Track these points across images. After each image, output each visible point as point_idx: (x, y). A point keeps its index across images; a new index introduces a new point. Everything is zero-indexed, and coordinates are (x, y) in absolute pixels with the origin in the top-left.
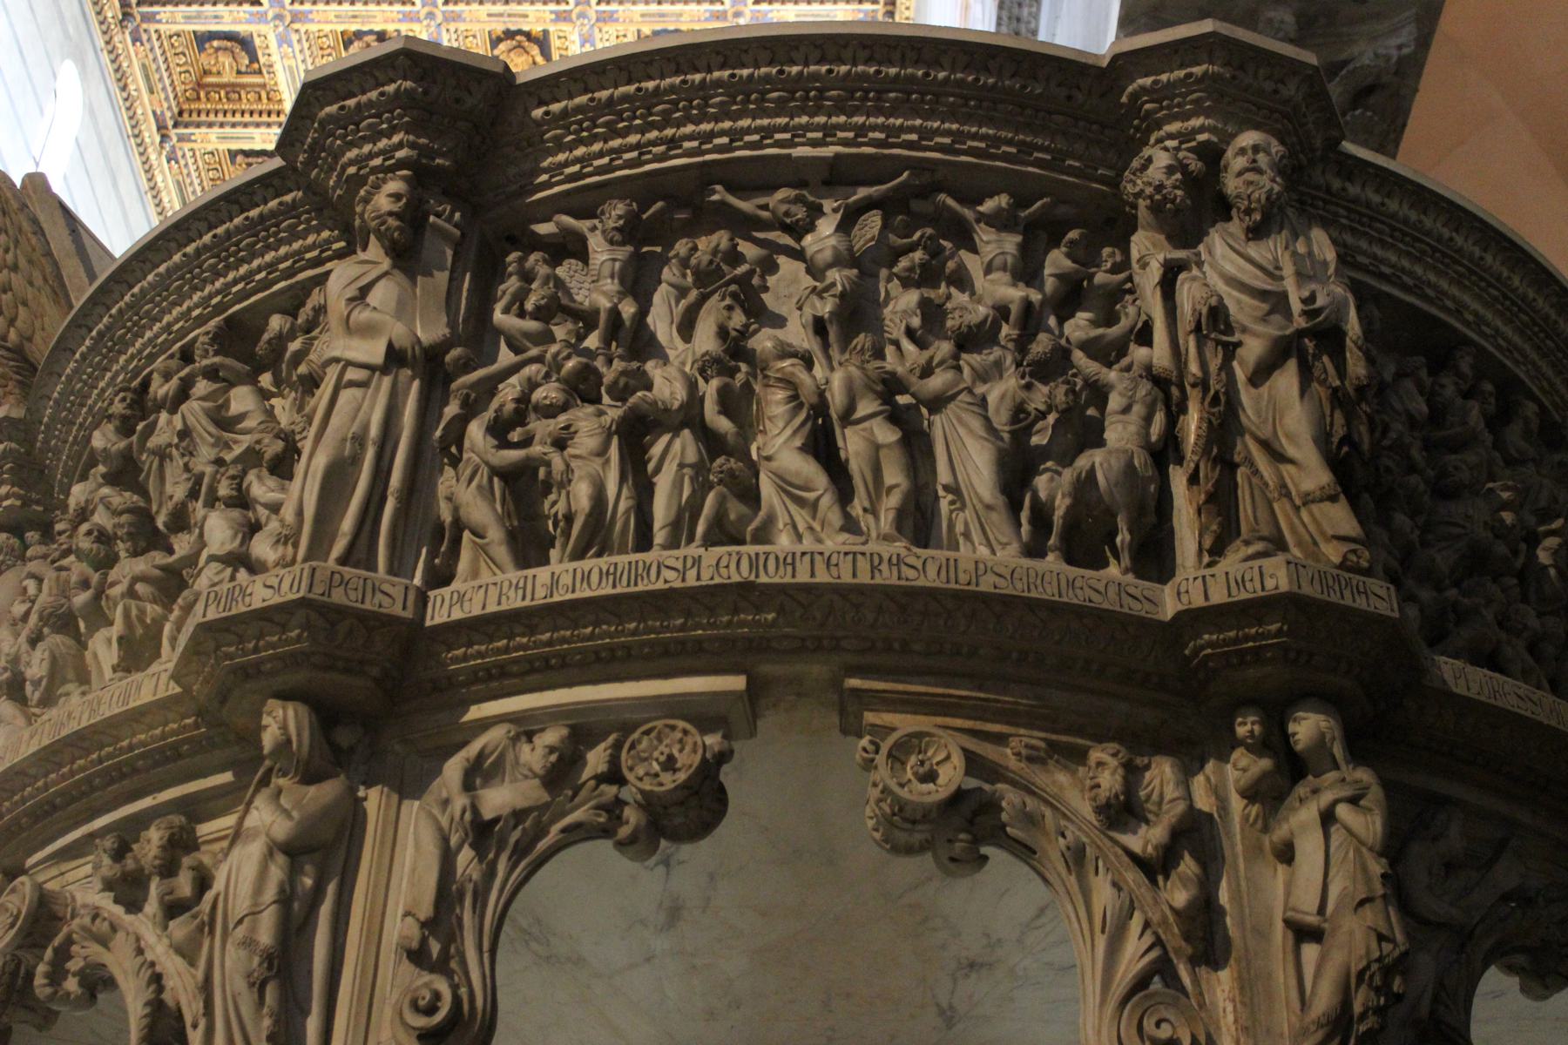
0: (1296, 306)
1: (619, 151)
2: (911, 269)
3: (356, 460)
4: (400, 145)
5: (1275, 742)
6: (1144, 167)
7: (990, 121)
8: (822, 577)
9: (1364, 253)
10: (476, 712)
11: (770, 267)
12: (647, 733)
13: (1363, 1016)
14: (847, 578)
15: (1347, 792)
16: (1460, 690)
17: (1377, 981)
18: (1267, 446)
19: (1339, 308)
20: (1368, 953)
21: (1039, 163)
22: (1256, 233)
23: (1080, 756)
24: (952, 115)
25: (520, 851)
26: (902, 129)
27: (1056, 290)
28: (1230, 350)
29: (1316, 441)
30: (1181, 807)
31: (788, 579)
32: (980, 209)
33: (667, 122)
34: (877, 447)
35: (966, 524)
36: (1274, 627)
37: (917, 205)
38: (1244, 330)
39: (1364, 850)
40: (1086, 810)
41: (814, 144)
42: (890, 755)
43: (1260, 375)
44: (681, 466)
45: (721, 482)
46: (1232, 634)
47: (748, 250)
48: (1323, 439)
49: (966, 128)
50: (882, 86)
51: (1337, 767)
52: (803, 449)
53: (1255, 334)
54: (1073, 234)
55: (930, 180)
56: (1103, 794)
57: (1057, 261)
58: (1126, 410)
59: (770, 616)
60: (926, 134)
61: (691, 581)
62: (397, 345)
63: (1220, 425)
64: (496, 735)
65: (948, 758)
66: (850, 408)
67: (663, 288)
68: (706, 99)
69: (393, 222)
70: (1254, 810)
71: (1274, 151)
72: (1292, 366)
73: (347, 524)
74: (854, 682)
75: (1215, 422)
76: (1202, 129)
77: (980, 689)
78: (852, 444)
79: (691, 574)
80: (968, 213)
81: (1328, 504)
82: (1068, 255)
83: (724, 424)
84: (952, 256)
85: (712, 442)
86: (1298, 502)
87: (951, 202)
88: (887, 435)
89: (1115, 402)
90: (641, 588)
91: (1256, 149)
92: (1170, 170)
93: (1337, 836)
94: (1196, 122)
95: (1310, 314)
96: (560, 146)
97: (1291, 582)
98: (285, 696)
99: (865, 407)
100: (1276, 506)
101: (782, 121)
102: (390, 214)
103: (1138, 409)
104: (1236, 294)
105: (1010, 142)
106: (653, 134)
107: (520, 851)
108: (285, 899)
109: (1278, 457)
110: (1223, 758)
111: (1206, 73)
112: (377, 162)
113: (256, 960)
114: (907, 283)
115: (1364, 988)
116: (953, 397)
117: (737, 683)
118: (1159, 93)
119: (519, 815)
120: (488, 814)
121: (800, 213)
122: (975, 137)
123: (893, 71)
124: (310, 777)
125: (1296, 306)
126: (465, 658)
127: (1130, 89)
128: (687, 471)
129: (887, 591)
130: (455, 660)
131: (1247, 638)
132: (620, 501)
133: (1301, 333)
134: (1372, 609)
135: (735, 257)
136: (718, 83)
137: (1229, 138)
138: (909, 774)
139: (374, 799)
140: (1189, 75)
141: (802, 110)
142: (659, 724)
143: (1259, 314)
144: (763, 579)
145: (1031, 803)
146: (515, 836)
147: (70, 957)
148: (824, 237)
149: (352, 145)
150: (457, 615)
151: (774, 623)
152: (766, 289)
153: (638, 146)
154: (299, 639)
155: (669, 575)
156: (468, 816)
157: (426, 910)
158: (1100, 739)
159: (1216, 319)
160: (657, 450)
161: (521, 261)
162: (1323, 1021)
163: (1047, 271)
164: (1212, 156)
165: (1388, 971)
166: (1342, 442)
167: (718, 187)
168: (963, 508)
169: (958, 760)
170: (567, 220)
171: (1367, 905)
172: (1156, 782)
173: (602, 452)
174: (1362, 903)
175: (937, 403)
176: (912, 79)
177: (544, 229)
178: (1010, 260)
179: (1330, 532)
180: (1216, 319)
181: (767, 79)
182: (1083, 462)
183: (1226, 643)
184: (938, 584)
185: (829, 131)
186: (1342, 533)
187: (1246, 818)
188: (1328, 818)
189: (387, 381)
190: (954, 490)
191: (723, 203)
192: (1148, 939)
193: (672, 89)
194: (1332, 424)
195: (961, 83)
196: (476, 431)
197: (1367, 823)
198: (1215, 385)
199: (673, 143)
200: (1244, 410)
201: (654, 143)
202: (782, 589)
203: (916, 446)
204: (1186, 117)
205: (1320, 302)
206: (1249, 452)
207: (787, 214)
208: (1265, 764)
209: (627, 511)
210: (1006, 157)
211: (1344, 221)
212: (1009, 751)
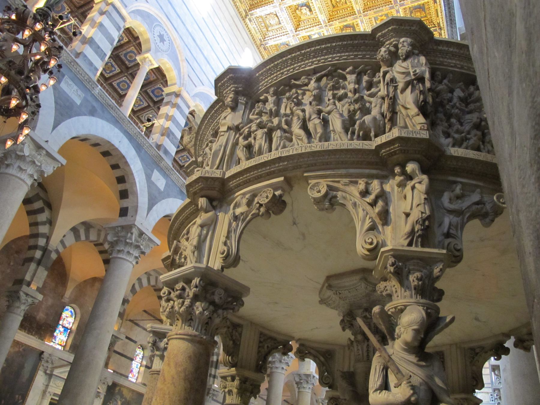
0: (412, 74)
1: (272, 78)
2: (330, 87)
3: (220, 150)
4: (232, 87)
5: (404, 173)
6: (380, 52)
7: (347, 52)
8: (295, 152)
9: (446, 62)
10: (237, 194)
11: (304, 94)
12: (264, 192)
13: (418, 231)
14: (300, 152)
15: (418, 181)
16: (456, 154)
17: (421, 223)
18: (403, 106)
19: (424, 72)
20: (418, 216)
21: (359, 58)
22: (405, 60)
23: (356, 183)
24: (338, 52)
25: (243, 220)
26: (328, 58)
27: (366, 85)
28: (396, 88)
29: (414, 103)
30: (378, 190)
31: (288, 154)
32: (346, 71)
33: (281, 69)
34: (315, 125)
35: (337, 138)
36: (397, 145)
37: (334, 74)
38: (399, 82)
39: (421, 194)
40: (358, 195)
41: (310, 66)
42: (310, 188)
43: (403, 90)
44: (277, 137)
45: (284, 139)
46: (388, 149)
47: (299, 92)
48: (416, 103)
49: (342, 54)
50: (322, 50)
51: (418, 176)
52: (300, 128)
53: (401, 82)
54: (369, 72)
55: (336, 67)
56: (360, 190)
57: (365, 78)
58: (375, 106)
59: (286, 163)
60: (333, 58)
61: (269, 159)
62: (229, 126)
63: (392, 104)
64: (239, 198)
65: (323, 187)
66: (310, 117)
67: (284, 103)
68: (287, 63)
69: (230, 103)
70: (400, 189)
71: (408, 41)
72: (410, 87)
73: (218, 162)
74: (305, 174)
75: (390, 103)
76: (394, 41)
77: (333, 171)
78: (310, 126)
79: (269, 157)
80: (344, 73)
81: (417, 116)
82: (368, 77)
83: (285, 127)
84: (342, 83)
85: (285, 131)
86: (411, 118)
87: (341, 71)
88: (317, 121)
89: (373, 105)
90: (260, 162)
91: (403, 42)
92: (385, 51)
93: (416, 191)
94: (392, 40)
95: (414, 75)
96: (263, 80)
97: (399, 134)
98: (202, 197)
99: (313, 117)
100: (406, 120)
101: (303, 63)
102: (230, 101)
103: (378, 106)
104: (399, 75)
105: (352, 55)
106: (278, 73)
107: (243, 220)
108: (200, 236)
109: (406, 108)
110: (394, 178)
111: (392, 28)
112: (228, 92)
113: (193, 247)
114: (330, 90)
115: (418, 225)
116: (333, 111)
117: (282, 179)
118: (383, 36)
119: (242, 214)
120: (237, 214)
121: (306, 81)
122: (344, 56)
123: (323, 46)
124: (206, 212)
125: (412, 74)
126: (233, 183)
127: (377, 36)
128: (279, 138)
129: (308, 153)
130: (231, 184)
131: (392, 149)
132: (265, 147)
133: (413, 80)
134: (421, 137)
136: (289, 59)
137: (399, 41)
138: (315, 192)
139: (221, 215)
140: (389, 30)
141: (307, 59)
142: (266, 190)
143: (403, 78)
144: (283, 155)
145: (344, 194)
146: (242, 217)
147: (182, 255)
148: (313, 84)
149: (225, 90)
150: (230, 175)
151: (287, 165)
152: (303, 99)
153: (276, 76)
154: (201, 185)
155: (265, 158)
156: (232, 215)
157: (226, 235)
158: (361, 178)
159: (393, 80)
160: (273, 136)
161: (258, 105)
162: (407, 233)
163: (364, 81)
164: (396, 46)
165: (424, 221)
166: (422, 101)
167: (292, 80)
168: (336, 135)
169: (326, 187)
170: (265, 95)
171: (419, 206)
172: (374, 186)
173: (262, 138)
174: (418, 205)
175: (329, 113)
176: (328, 47)
177: (262, 98)
178: (353, 80)
179: (418, 122)
180: (393, 80)
181: (298, 55)
182: (363, 119)
183: (387, 151)
184: (319, 149)
185: (312, 62)
186: (420, 122)
187: (398, 191)
188: (413, 188)
189: (228, 133)
190: (334, 131)
191: (294, 84)
192: (370, 220)
193: (281, 62)
194: (420, 98)
195: (339, 45)
196: (241, 139)
197: (422, 188)
198: (391, 95)
199: (282, 73)
200: (399, 99)
201: (279, 75)
202: (287, 157)
203: (325, 122)
204: (390, 39)
205: (417, 72)
206: (399, 108)
207: (304, 82)
208: (402, 178)
209: (266, 149)
210: (352, 59)
211: (439, 56)
212: (340, 184)
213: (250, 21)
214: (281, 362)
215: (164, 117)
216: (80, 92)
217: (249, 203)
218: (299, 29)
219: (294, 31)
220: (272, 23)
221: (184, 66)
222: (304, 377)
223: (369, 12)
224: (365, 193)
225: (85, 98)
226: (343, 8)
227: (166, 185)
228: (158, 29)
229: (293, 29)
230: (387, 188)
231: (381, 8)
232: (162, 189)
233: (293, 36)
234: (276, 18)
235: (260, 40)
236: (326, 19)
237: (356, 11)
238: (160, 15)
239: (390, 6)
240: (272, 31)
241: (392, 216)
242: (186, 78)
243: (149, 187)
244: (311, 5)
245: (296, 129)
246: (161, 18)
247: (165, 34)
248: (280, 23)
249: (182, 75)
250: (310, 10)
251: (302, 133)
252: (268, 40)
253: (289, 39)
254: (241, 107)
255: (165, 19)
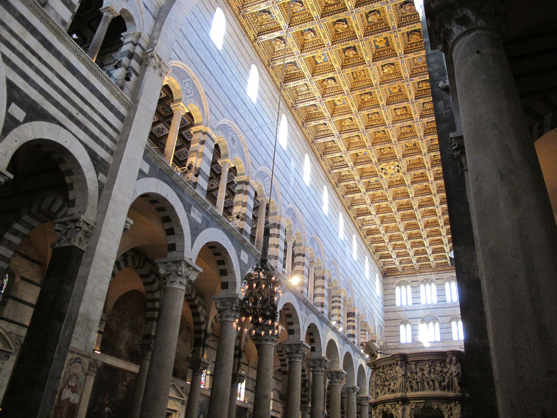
5: (455, 403)
88: (432, 383)
135: (422, 366)
159: (452, 373)
197: (460, 408)
213: (284, 90)
214: (321, 366)
215: (240, 204)
216: (200, 214)
217: (416, 406)
218: (325, 95)
219: (321, 97)
220: (302, 90)
221: (248, 156)
222: (335, 374)
223: (384, 85)
224: (447, 408)
225: (203, 216)
226: (363, 80)
227: (249, 259)
228: (231, 133)
229: (320, 96)
230: (451, 405)
231: (394, 82)
232: (246, 263)
233: (320, 101)
234: (306, 87)
235: (292, 103)
236: (348, 90)
237: (374, 84)
238: (231, 123)
239: (402, 81)
240: (301, 95)
241: (453, 414)
242: (250, 165)
243: (240, 265)
244: (336, 78)
245: (426, 384)
246: (232, 124)
247: (235, 137)
248: (308, 90)
249: (247, 164)
250: (335, 81)
251: (427, 386)
252: (299, 103)
253: (316, 103)
254: (403, 366)
255: (234, 124)
